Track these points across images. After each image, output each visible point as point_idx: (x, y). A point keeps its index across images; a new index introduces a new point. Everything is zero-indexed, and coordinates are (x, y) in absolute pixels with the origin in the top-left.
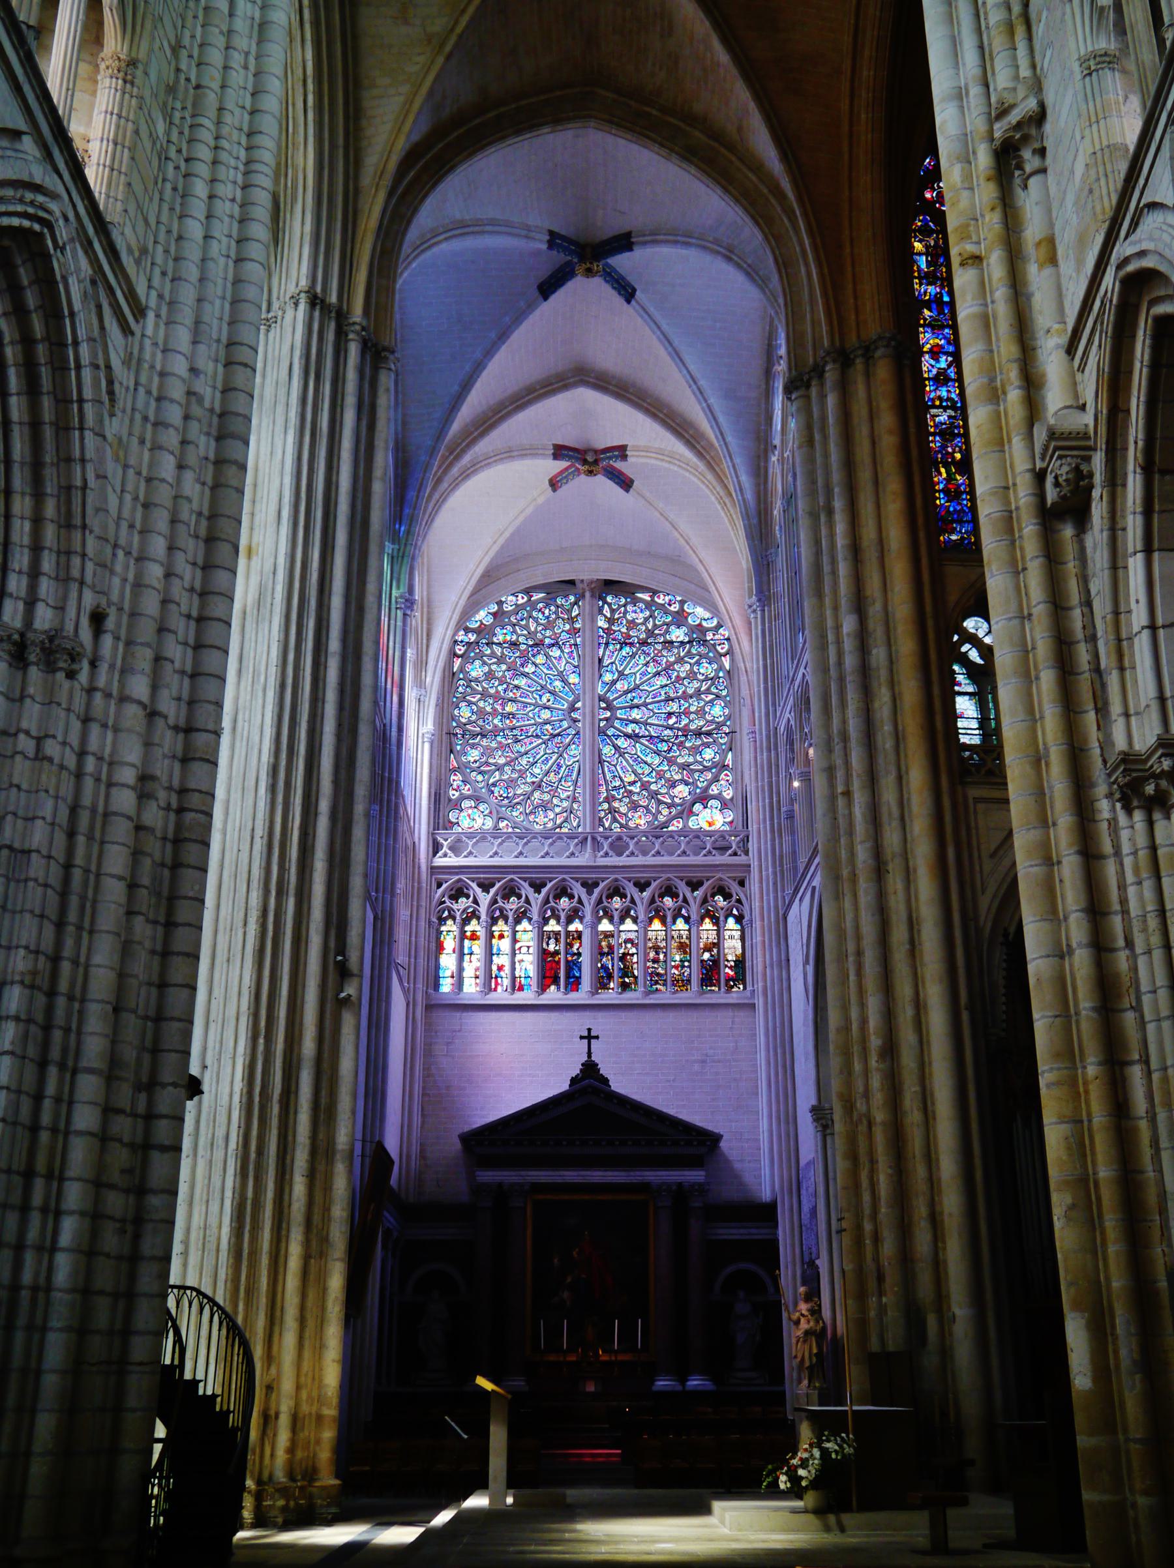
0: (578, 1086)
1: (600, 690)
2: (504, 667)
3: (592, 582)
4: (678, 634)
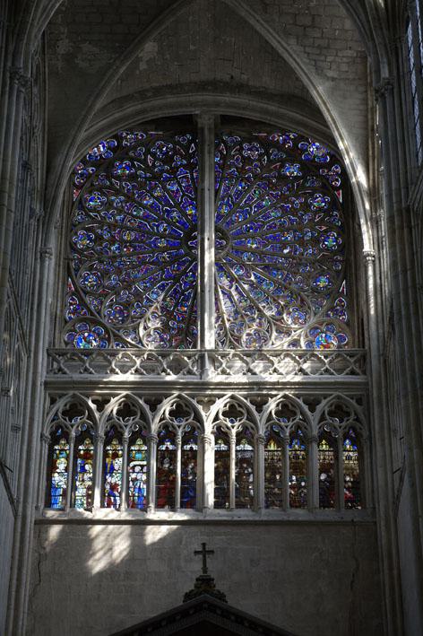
0: (193, 601)
4: (293, 171)
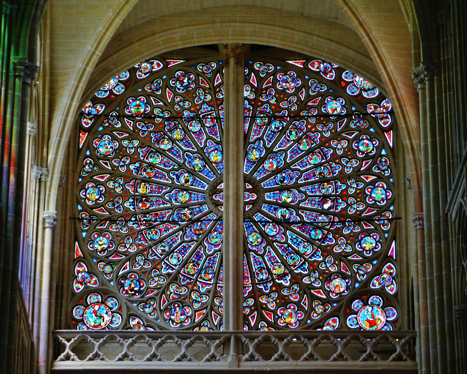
1: (246, 170)
2: (136, 143)
3: (237, 47)
